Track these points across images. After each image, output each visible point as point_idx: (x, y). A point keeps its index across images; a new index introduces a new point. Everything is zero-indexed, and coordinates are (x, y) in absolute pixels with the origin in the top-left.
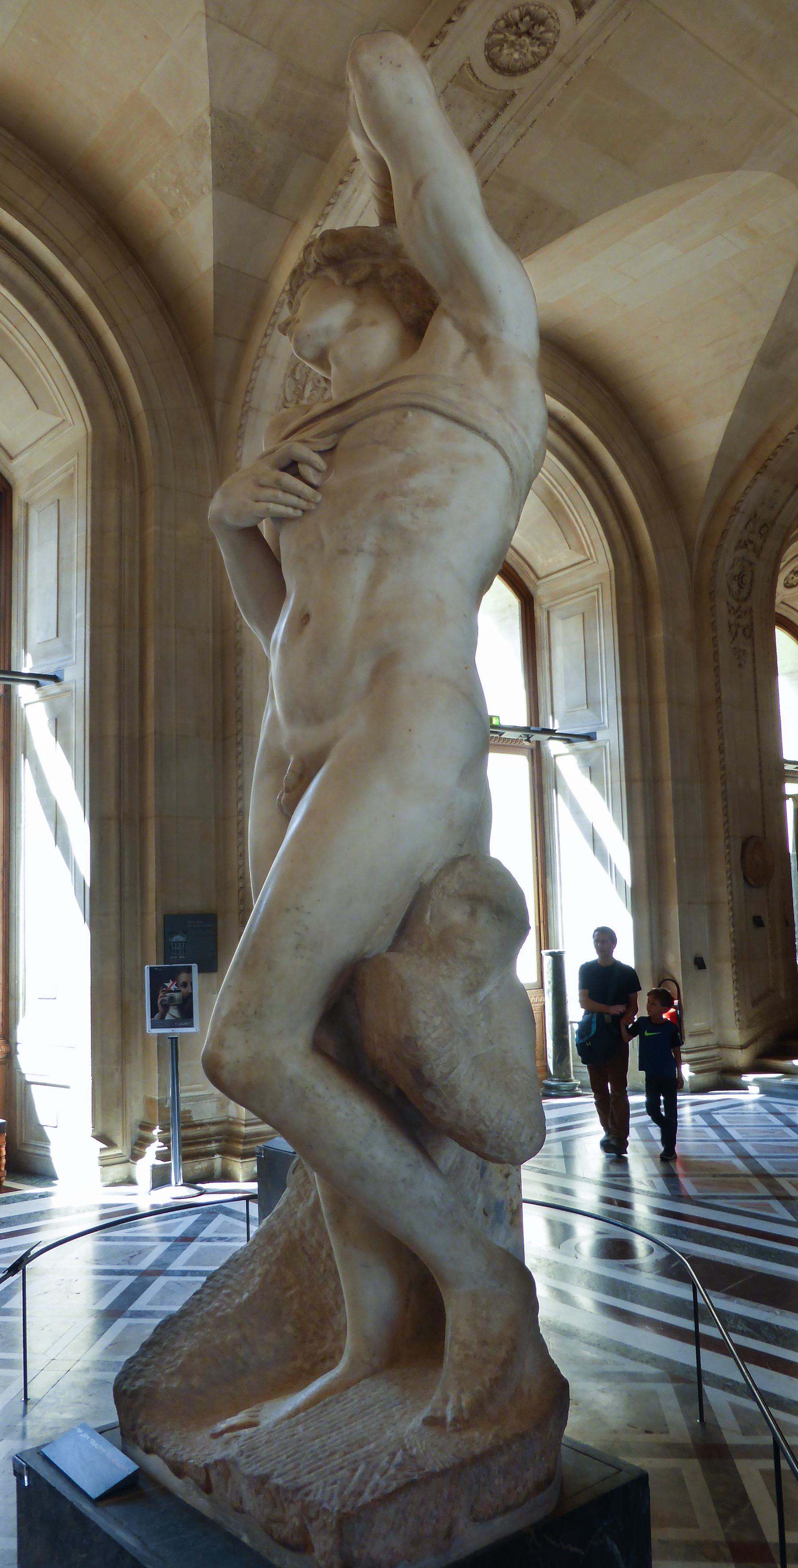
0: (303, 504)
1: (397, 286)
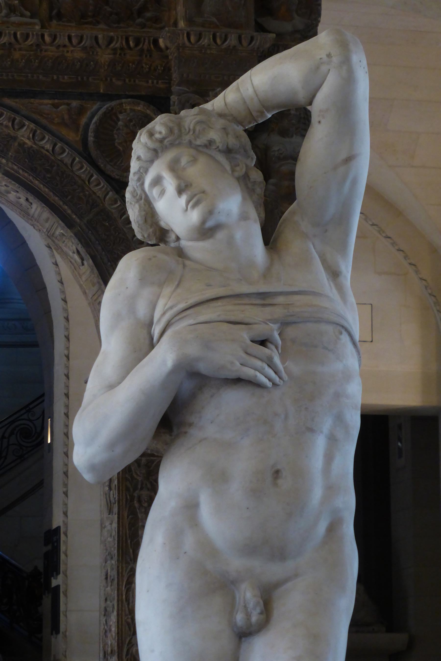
0: (277, 379)
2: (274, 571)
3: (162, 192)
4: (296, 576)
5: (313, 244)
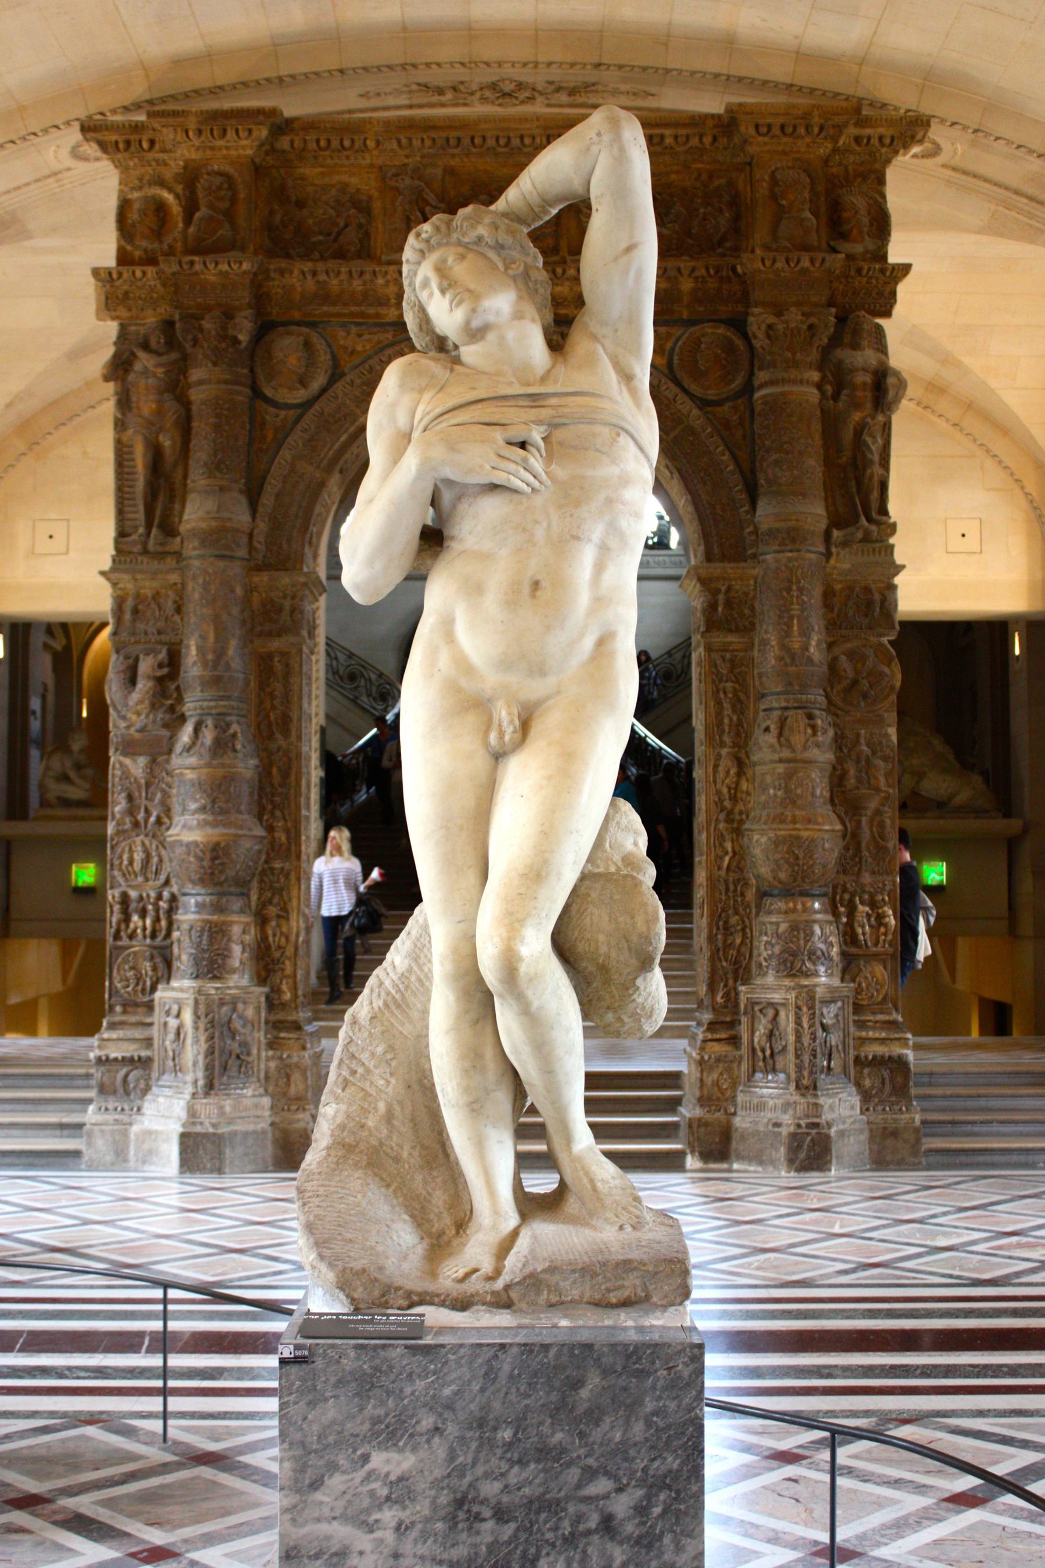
0: (536, 484)
1: (541, 290)
2: (534, 689)
3: (431, 295)
4: (559, 692)
5: (603, 347)
